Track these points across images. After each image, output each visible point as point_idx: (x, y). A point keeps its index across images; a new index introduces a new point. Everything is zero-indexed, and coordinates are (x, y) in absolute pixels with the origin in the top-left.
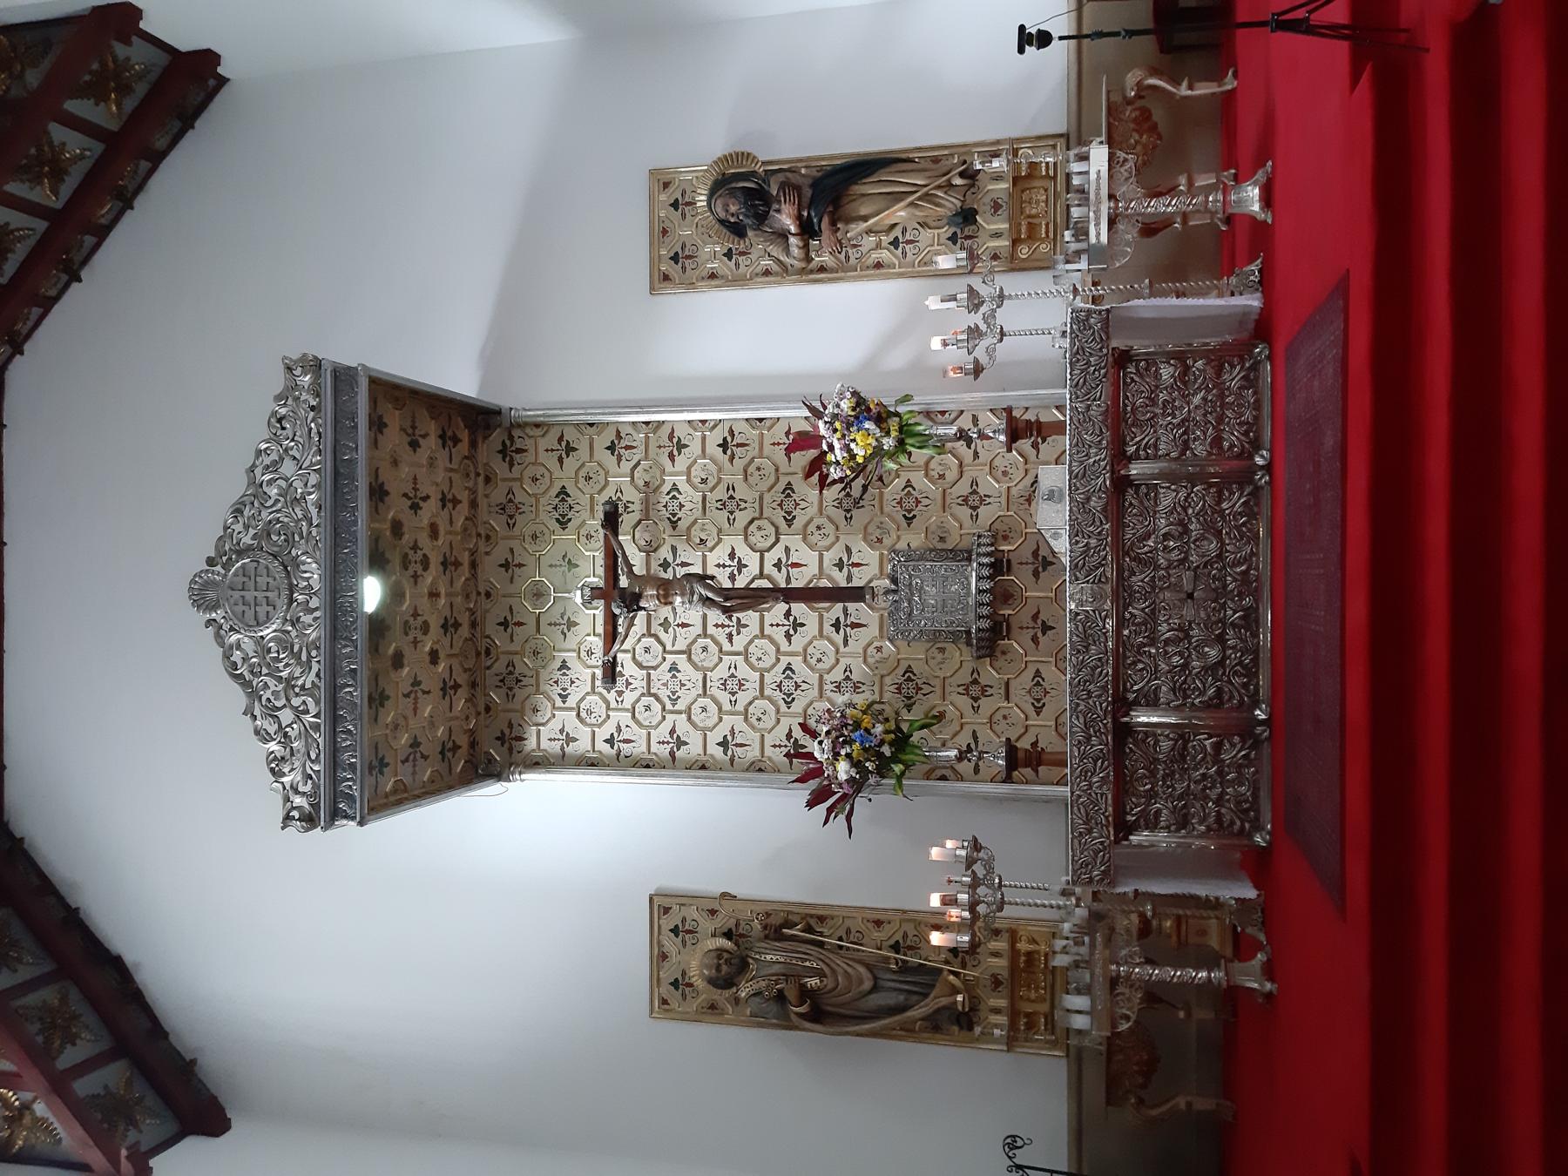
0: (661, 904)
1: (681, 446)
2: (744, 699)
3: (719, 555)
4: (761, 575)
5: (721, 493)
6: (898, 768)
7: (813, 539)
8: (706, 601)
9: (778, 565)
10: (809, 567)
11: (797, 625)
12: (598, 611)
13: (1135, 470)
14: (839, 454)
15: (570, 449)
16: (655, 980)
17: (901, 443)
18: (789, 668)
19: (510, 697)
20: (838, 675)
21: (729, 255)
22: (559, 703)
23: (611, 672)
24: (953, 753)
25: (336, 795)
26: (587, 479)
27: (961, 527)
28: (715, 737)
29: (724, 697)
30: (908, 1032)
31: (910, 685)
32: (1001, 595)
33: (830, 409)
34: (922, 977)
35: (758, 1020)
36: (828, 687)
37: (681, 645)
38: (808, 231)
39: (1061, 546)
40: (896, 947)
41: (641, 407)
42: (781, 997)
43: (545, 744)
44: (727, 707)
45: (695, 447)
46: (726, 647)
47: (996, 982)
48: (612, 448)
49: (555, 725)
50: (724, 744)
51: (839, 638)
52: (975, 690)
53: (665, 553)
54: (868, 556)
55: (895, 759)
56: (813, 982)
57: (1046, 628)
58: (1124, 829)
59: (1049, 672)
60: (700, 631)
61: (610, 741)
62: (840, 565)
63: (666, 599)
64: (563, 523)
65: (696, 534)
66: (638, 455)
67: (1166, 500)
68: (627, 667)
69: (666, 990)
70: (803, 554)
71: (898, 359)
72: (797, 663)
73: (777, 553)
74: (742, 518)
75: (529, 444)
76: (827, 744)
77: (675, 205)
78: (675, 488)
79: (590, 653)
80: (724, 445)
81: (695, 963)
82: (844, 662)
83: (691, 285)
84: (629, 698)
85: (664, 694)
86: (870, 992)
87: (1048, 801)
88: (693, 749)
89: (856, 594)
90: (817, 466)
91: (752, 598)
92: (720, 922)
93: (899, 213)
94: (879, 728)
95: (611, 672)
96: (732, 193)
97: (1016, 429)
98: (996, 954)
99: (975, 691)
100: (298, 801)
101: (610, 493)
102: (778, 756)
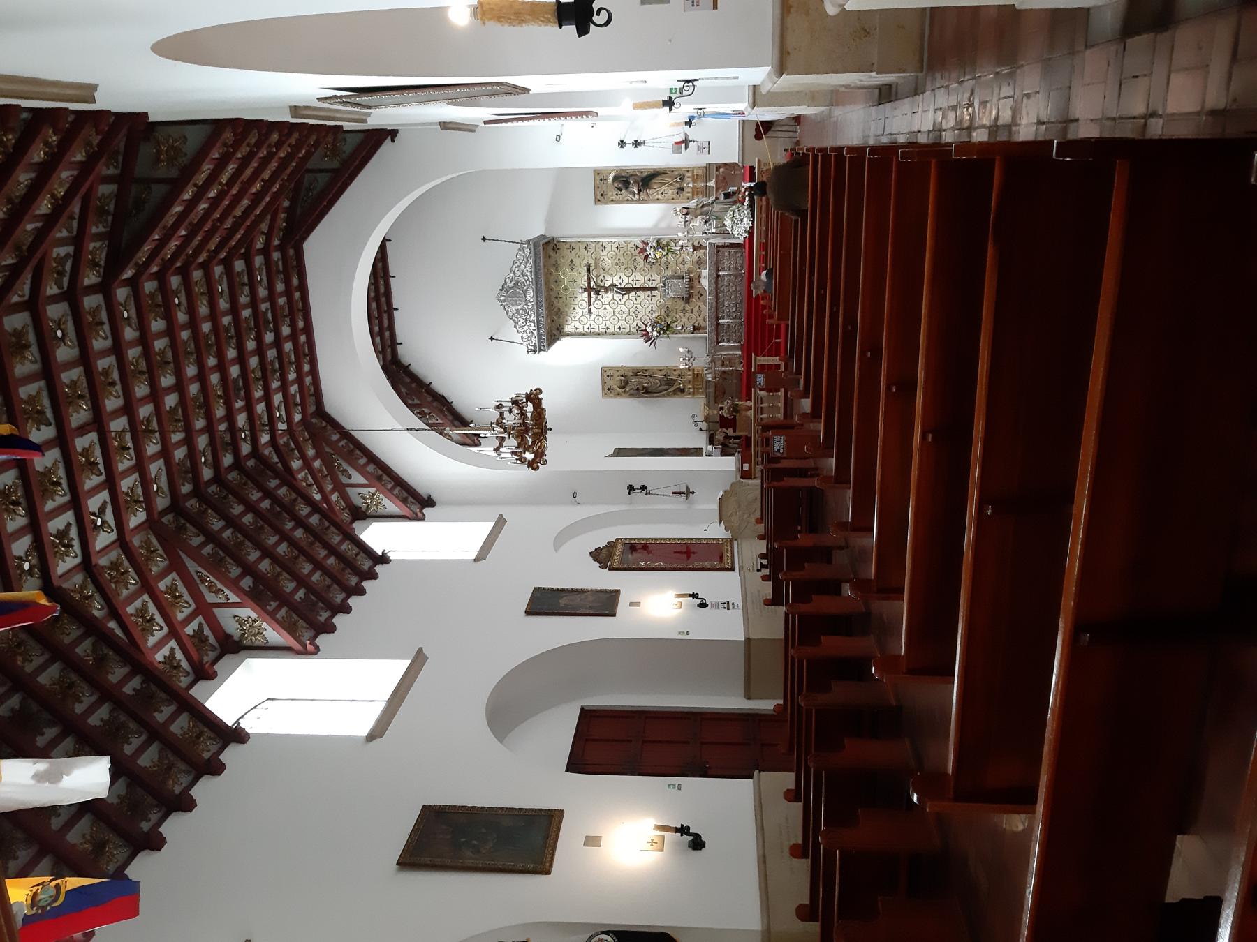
0: (604, 370)
1: (605, 248)
2: (624, 316)
3: (617, 278)
4: (628, 283)
5: (617, 261)
6: (668, 332)
7: (642, 273)
8: (617, 292)
9: (633, 280)
10: (641, 280)
11: (638, 296)
12: (586, 294)
13: (721, 273)
14: (652, 256)
15: (573, 248)
16: (603, 389)
17: (667, 254)
18: (636, 307)
19: (559, 317)
20: (649, 309)
21: (617, 194)
22: (573, 319)
23: (590, 312)
24: (680, 328)
25: (540, 346)
26: (579, 257)
27: (681, 270)
28: (617, 327)
29: (619, 316)
30: (668, 395)
31: (668, 311)
32: (691, 287)
33: (650, 244)
34: (671, 382)
35: (632, 395)
36: (647, 312)
37: (607, 302)
38: (639, 191)
39: (707, 288)
40: (665, 376)
41: (594, 237)
42: (638, 389)
43: (570, 330)
44: (620, 318)
45: (609, 248)
46: (619, 302)
47: (689, 382)
48: (585, 248)
49: (573, 325)
50: (620, 328)
51: (649, 299)
52: (684, 311)
53: (601, 277)
54: (657, 278)
55: (667, 330)
56: (646, 385)
57: (701, 295)
58: (718, 343)
59: (702, 306)
60: (612, 298)
61: (588, 328)
62: (649, 280)
63: (606, 292)
64: (572, 269)
65: (610, 272)
66: (593, 250)
67: (726, 279)
68: (593, 309)
69: (606, 391)
70: (639, 277)
71: (663, 225)
72: (639, 306)
73: (633, 277)
74: (623, 268)
75: (561, 247)
76: (650, 328)
77: (601, 180)
78: (604, 259)
79: (581, 305)
80: (617, 248)
81: (614, 382)
82: (651, 306)
83: (606, 203)
84: (593, 317)
85: (602, 315)
86: (659, 386)
87: (701, 338)
88: (611, 330)
89: (655, 288)
90: (646, 257)
91: (629, 290)
92: (619, 373)
93: (664, 187)
94: (663, 323)
95: (590, 312)
96: (620, 182)
97: (695, 248)
98: (689, 375)
99: (684, 311)
100: (530, 347)
101: (585, 262)
102: (634, 330)
